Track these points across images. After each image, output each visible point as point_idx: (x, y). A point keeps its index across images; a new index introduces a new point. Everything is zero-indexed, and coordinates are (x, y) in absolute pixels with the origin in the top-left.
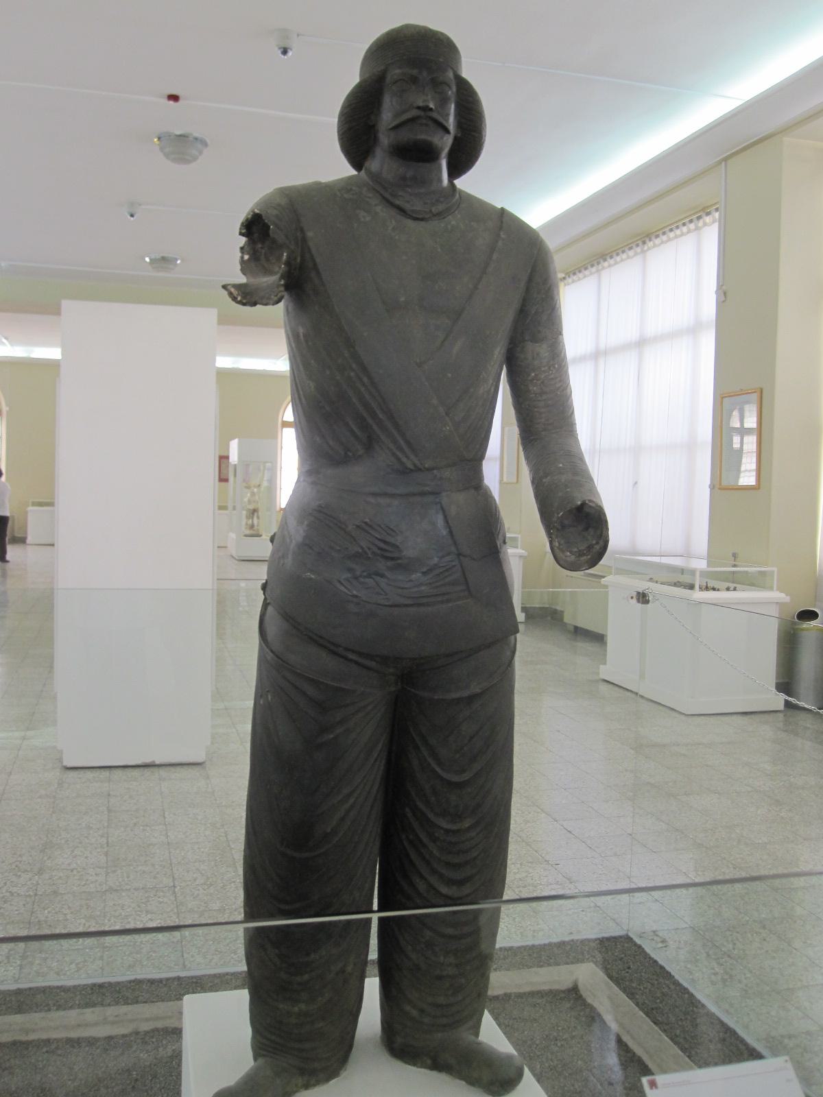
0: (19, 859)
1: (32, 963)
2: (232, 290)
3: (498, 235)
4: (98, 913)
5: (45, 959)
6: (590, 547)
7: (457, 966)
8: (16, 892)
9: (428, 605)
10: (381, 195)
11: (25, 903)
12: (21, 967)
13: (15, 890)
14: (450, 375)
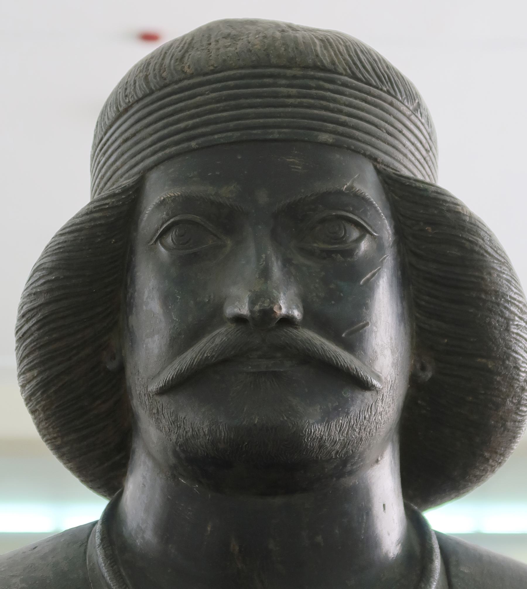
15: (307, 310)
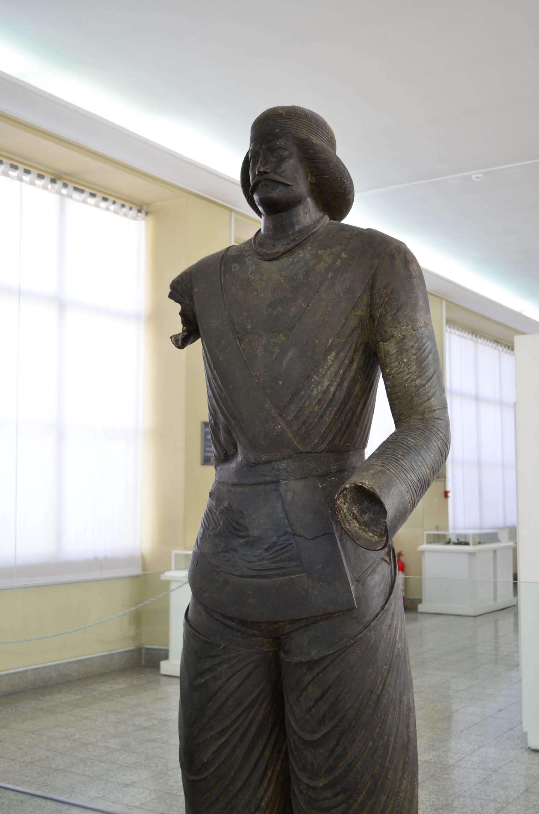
9: (266, 577)
14: (281, 383)
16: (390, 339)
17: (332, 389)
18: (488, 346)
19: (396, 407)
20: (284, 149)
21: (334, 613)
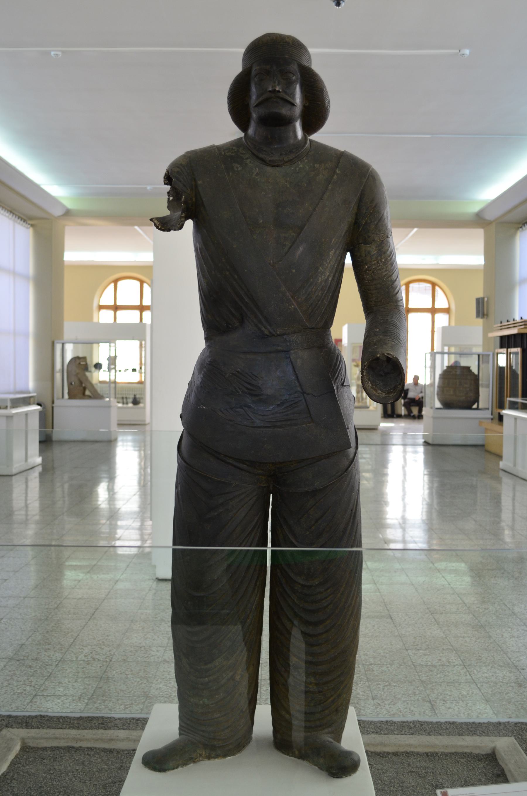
0: (106, 638)
1: (95, 703)
2: (156, 222)
3: (335, 172)
4: (151, 675)
5: (104, 701)
6: (395, 388)
7: (316, 684)
8: (97, 659)
10: (251, 151)
11: (101, 665)
12: (87, 704)
13: (97, 657)
15: (283, 90)
16: (372, 242)
17: (330, 279)
18: (5, 216)
19: (374, 295)
20: (293, 74)
21: (334, 453)
